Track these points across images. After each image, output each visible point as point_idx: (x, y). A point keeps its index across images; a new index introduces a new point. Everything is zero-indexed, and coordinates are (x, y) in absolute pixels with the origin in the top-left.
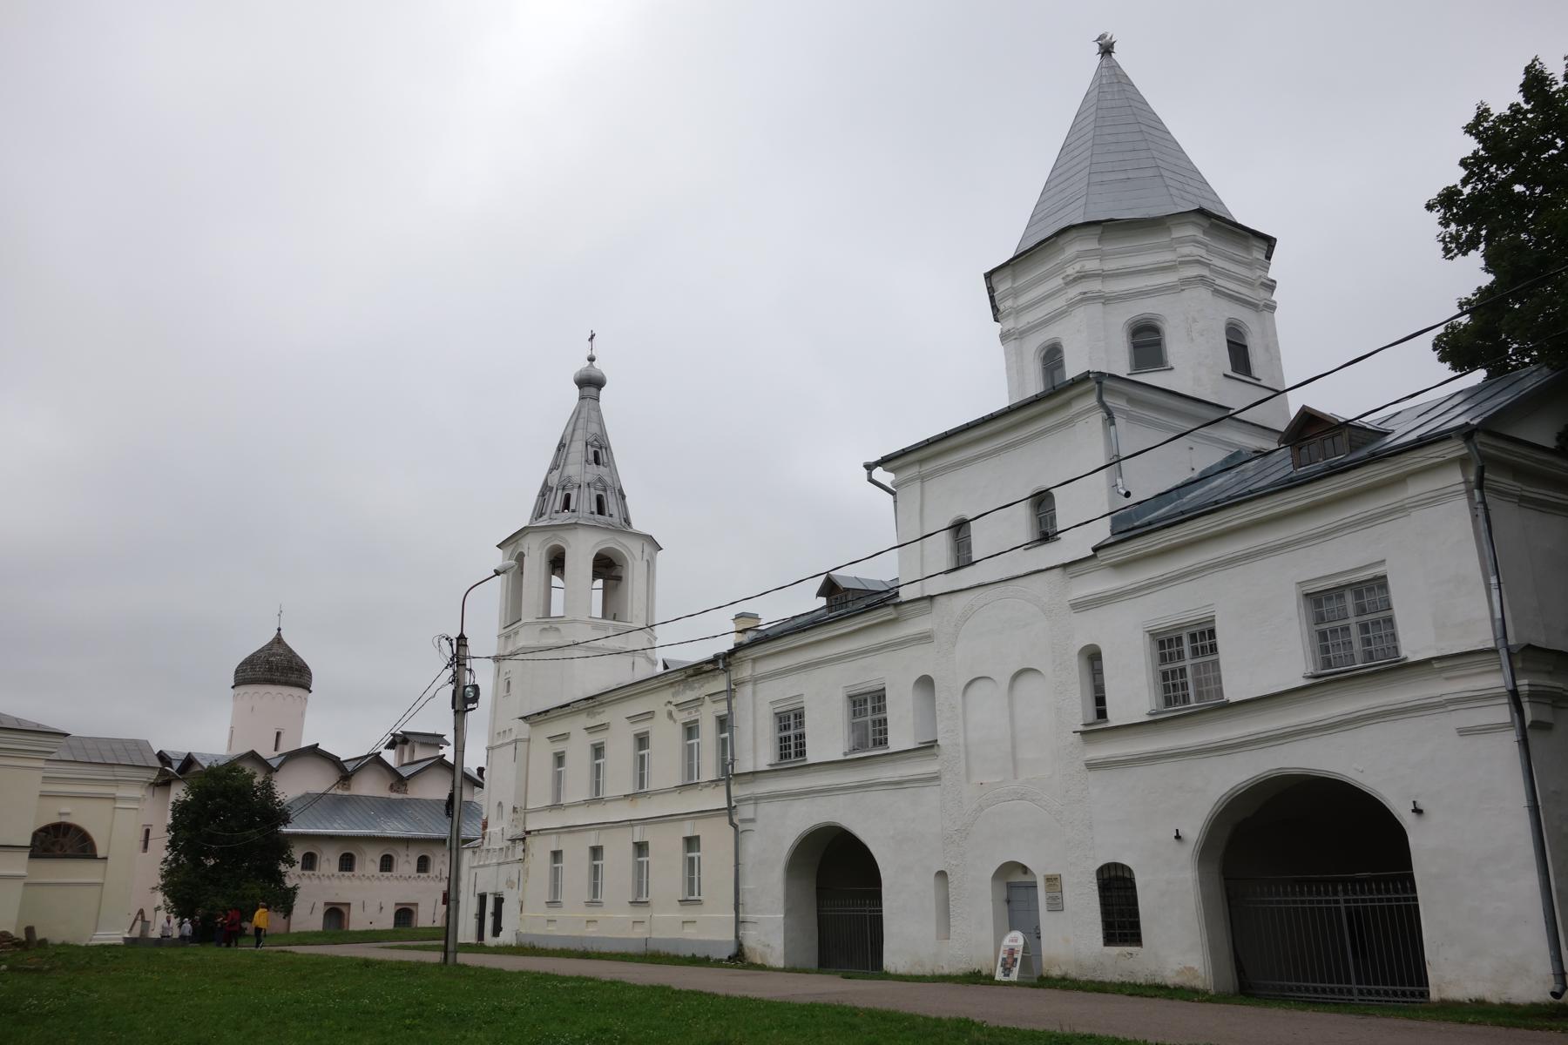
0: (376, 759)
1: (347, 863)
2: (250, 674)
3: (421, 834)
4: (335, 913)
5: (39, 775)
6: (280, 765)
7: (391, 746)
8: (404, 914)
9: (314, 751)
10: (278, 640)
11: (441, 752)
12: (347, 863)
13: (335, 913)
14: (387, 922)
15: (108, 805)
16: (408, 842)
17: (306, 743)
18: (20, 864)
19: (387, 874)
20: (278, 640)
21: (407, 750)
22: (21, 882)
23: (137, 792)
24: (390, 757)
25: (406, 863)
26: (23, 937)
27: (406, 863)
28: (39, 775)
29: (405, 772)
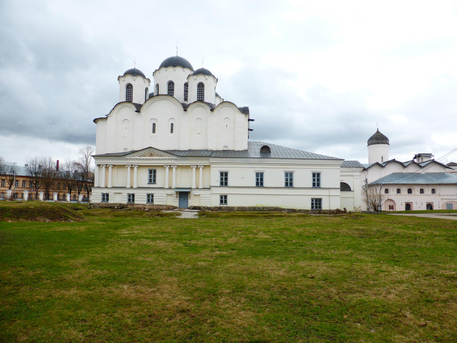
0: (413, 162)
1: (410, 191)
2: (372, 142)
3: (432, 183)
4: (408, 206)
5: (339, 170)
6: (385, 166)
7: (415, 158)
8: (430, 206)
9: (394, 161)
10: (378, 132)
11: (432, 159)
12: (410, 191)
13: (408, 206)
14: (424, 208)
15: (352, 177)
16: (428, 185)
17: (390, 159)
18: (338, 192)
19: (422, 194)
20: (378, 132)
21: (420, 159)
22: (339, 197)
23: (358, 174)
24: (415, 160)
25: (428, 191)
26: (343, 210)
27: (428, 191)
28: (339, 170)
29: (422, 165)
